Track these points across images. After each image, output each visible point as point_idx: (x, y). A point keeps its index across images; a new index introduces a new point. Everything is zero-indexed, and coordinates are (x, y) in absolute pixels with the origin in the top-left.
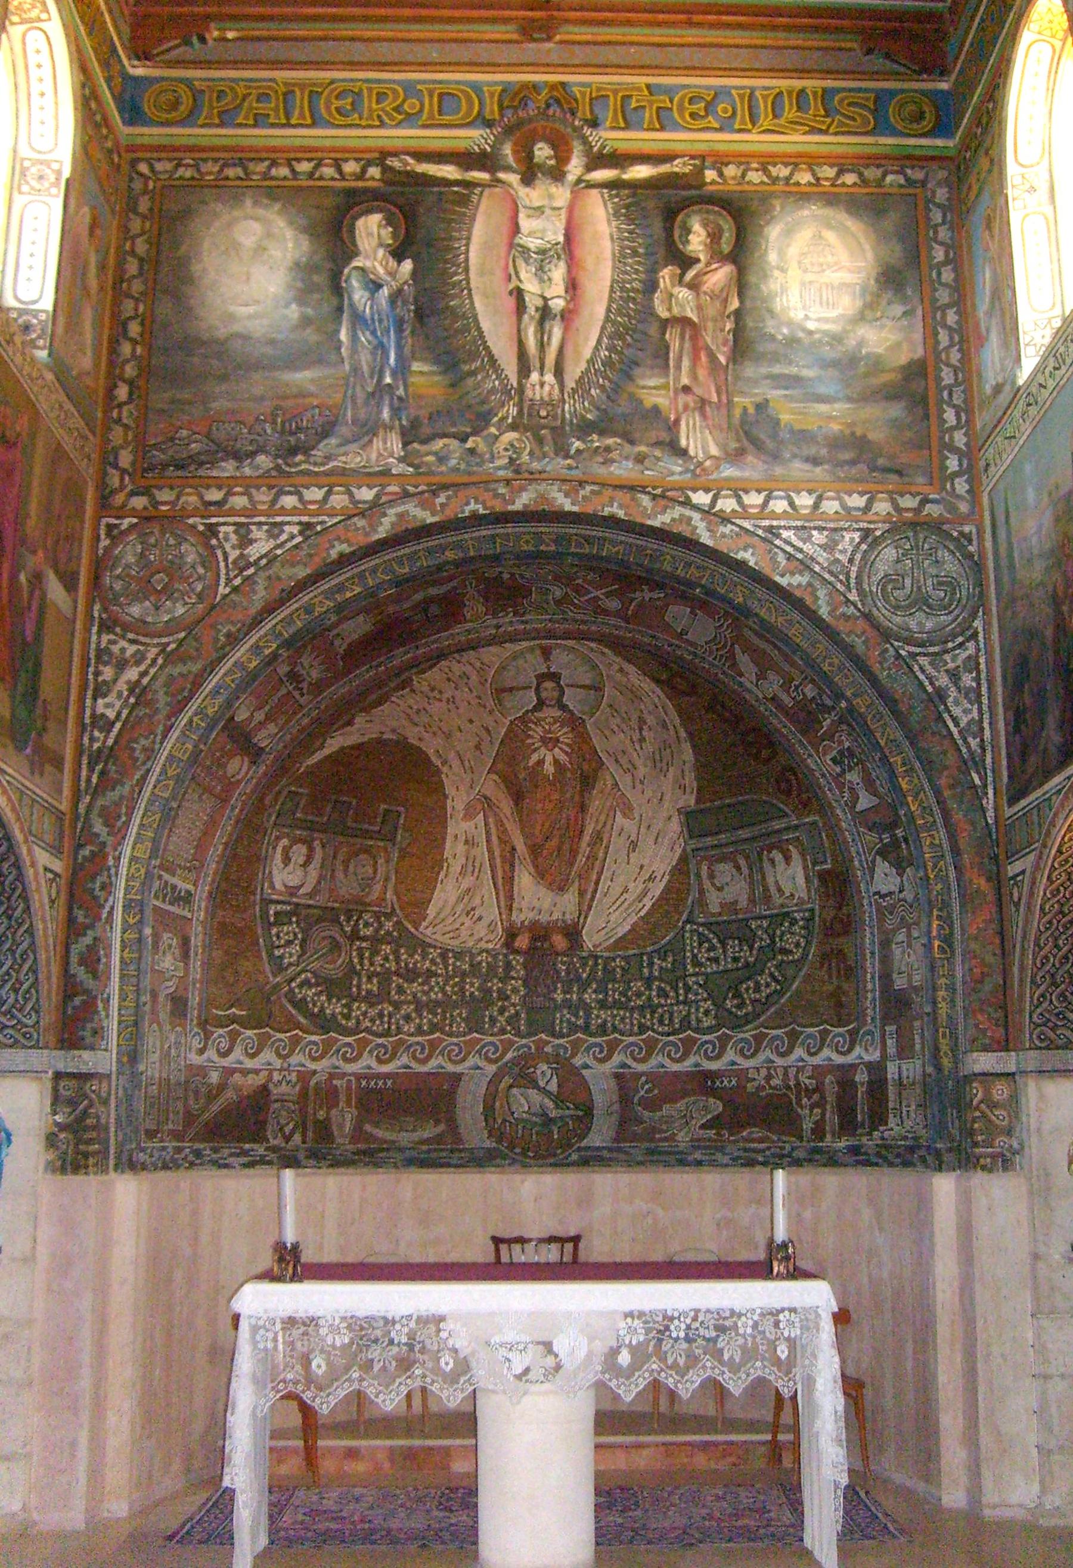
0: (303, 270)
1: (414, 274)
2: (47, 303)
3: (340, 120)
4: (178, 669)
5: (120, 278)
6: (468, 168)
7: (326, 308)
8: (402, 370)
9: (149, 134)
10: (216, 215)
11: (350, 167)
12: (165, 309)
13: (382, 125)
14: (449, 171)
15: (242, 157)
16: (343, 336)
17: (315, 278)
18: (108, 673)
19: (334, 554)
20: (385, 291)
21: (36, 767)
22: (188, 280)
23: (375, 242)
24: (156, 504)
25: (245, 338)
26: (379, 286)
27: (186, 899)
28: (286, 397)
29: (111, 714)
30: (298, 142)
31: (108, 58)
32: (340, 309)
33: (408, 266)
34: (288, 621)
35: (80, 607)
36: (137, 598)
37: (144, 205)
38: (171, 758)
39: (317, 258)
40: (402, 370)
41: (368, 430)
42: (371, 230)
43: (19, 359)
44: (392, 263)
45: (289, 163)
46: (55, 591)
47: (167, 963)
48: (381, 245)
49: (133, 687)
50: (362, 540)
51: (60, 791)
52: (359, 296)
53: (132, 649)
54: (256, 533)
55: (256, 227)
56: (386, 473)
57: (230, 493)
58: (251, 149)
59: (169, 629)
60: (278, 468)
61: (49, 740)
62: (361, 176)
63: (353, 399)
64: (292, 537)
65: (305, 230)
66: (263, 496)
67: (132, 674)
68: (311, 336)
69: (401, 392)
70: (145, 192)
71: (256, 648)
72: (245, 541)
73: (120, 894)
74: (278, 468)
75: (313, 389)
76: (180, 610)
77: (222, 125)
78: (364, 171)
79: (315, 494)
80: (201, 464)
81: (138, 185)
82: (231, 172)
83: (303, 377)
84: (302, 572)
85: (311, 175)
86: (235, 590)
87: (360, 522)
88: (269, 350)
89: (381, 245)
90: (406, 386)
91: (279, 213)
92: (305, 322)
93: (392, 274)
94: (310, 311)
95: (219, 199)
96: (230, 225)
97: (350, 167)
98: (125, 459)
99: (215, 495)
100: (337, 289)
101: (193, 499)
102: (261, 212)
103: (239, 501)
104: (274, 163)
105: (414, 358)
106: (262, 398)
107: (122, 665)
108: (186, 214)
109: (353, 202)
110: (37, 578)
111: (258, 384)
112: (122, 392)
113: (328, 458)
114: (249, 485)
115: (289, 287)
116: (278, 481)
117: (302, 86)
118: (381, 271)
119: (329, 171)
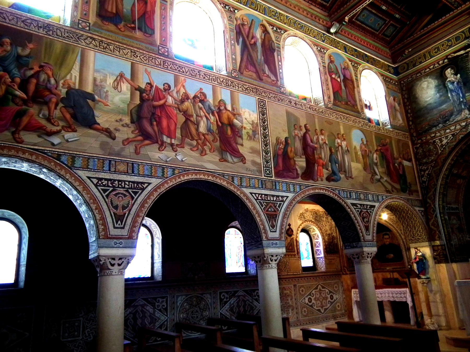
0: (437, 87)
1: (461, 77)
2: (388, 117)
3: (436, 54)
4: (435, 169)
5: (404, 103)
6: (466, 50)
7: (444, 92)
8: (464, 97)
9: (401, 76)
10: (418, 84)
11: (441, 62)
12: (414, 105)
13: (445, 51)
14: (462, 52)
15: (419, 71)
16: (449, 95)
17: (440, 87)
18: (423, 173)
19: (460, 138)
20: (456, 83)
21: (411, 193)
22: (416, 98)
23: (450, 74)
24: (422, 140)
25: (430, 104)
26: (453, 82)
27: (457, 208)
28: (441, 112)
29: (425, 180)
30: (429, 63)
31: (387, 69)
32: (447, 91)
33: (459, 75)
34: (457, 152)
35: (414, 163)
36: (425, 158)
37: (404, 89)
38: (441, 184)
39: (440, 83)
40: (464, 97)
41: (460, 111)
42: (449, 72)
43: (383, 131)
44: (455, 77)
45: (428, 68)
46: (406, 163)
47: (454, 222)
48: (452, 74)
49: (428, 174)
50: (465, 133)
51: (419, 196)
52: (450, 86)
53: (426, 168)
54: (443, 139)
55: (426, 83)
56: (467, 118)
57: (436, 134)
58: (421, 69)
59: (432, 161)
60: (444, 126)
61: (413, 188)
62: (444, 63)
63: (455, 107)
64: (450, 137)
65: (435, 79)
66: (442, 132)
67: (427, 172)
68: (443, 98)
69: (465, 101)
70: (404, 86)
71: (452, 160)
72: (441, 141)
73: (438, 211)
74: (444, 126)
75: (446, 108)
76: (433, 158)
77: (414, 67)
78: (444, 61)
79: (453, 128)
80: (429, 130)
81: (402, 86)
82: (418, 75)
83: (444, 106)
84: (454, 143)
85: (433, 68)
86: (442, 151)
87: (464, 130)
88: (435, 104)
89: (452, 74)
90: (466, 99)
91: (430, 78)
92: (441, 96)
93: (456, 79)
94: (441, 94)
95: (417, 81)
96: (421, 85)
97: (441, 62)
98: (415, 134)
99: (433, 135)
100: (445, 87)
101: (429, 137)
102: (426, 80)
103: (438, 134)
104: (426, 69)
105: (466, 93)
106: (437, 114)
107: (424, 171)
108: (413, 86)
109: (444, 68)
110: (400, 163)
111: (435, 112)
112: (411, 123)
113: (453, 120)
114: (439, 131)
115: (435, 91)
116: (444, 128)
117: (426, 52)
118: (453, 79)
119: (437, 65)
